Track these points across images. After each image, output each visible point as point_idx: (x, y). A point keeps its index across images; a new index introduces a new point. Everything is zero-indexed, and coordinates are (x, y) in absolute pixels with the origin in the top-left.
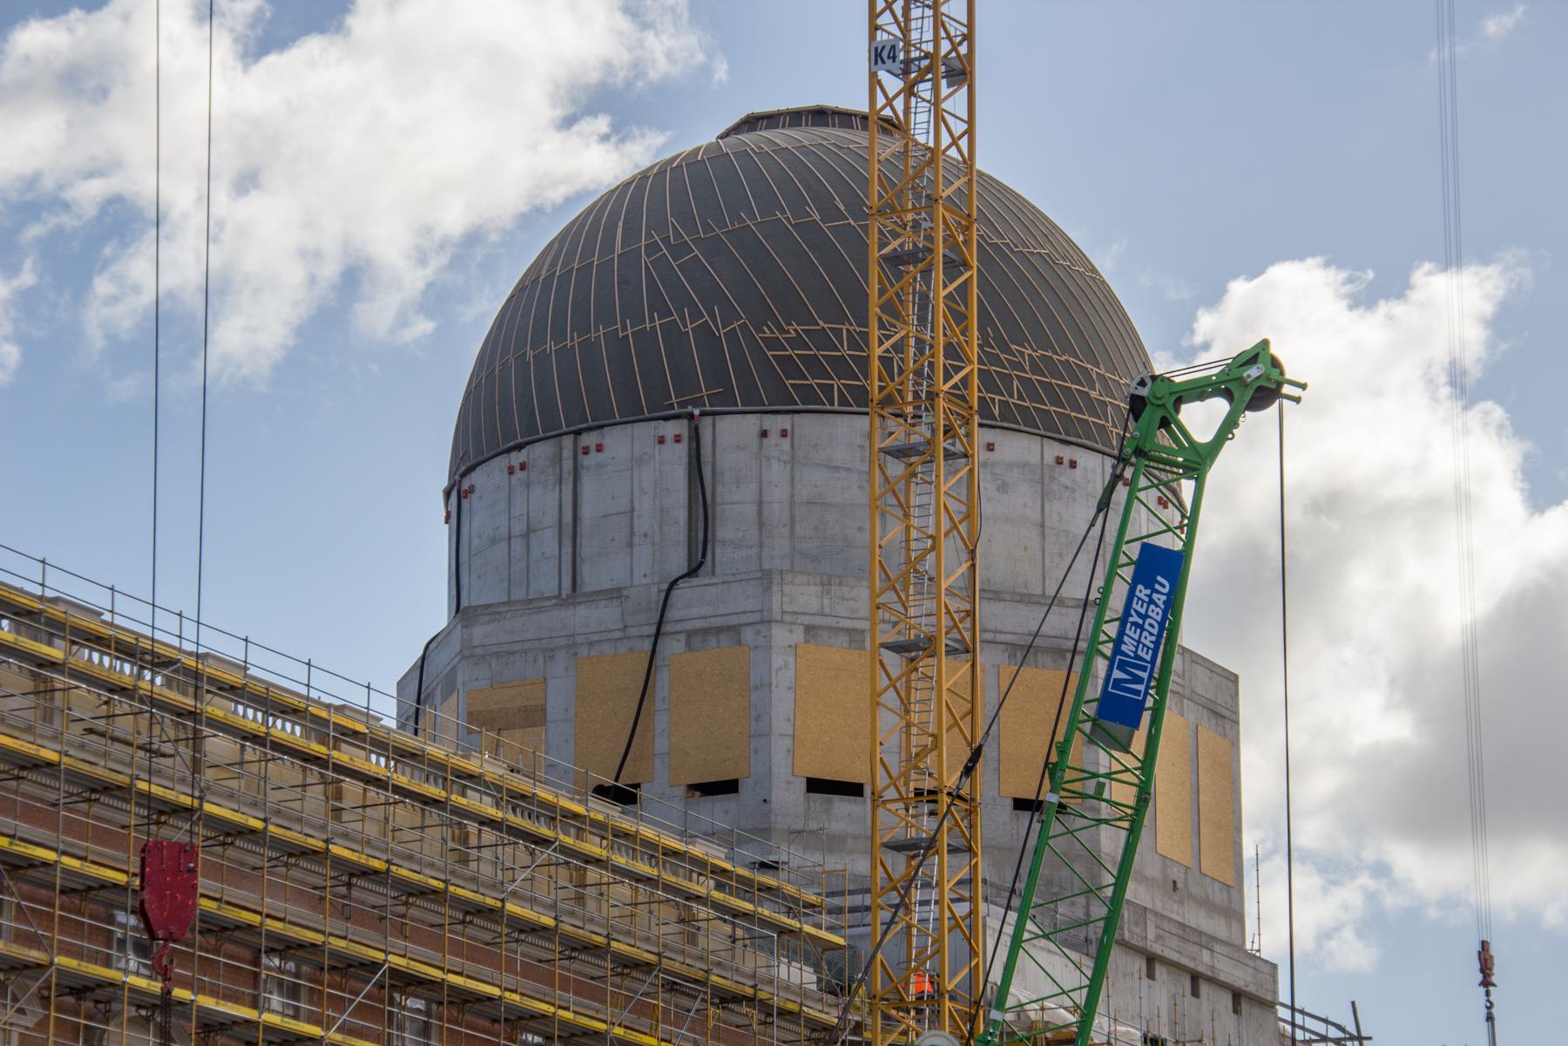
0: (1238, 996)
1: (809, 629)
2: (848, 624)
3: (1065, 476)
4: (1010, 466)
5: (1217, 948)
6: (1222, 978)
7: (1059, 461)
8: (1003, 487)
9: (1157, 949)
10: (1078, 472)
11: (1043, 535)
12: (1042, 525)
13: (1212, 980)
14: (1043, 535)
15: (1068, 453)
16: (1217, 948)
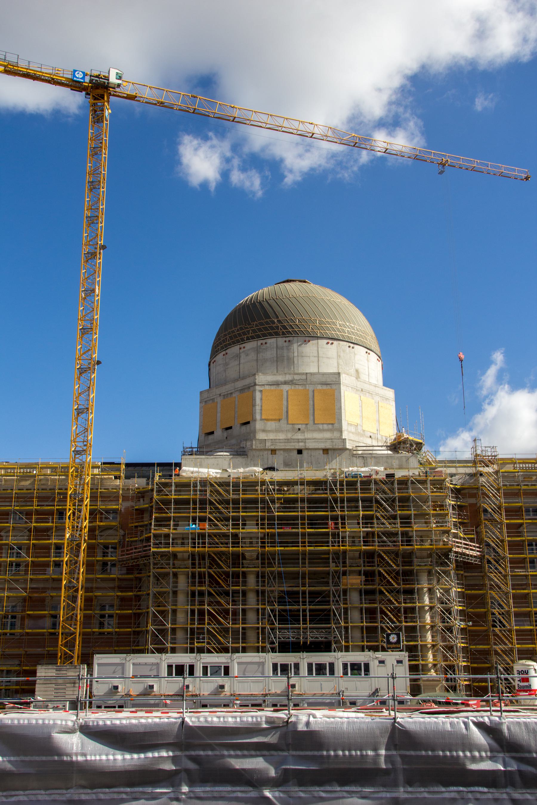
0: (326, 451)
1: (206, 402)
2: (212, 398)
3: (264, 347)
4: (249, 350)
5: (307, 441)
6: (311, 447)
7: (262, 344)
8: (247, 355)
9: (272, 447)
10: (268, 345)
11: (257, 362)
12: (257, 360)
13: (307, 449)
14: (257, 362)
15: (264, 342)
16: (307, 441)
